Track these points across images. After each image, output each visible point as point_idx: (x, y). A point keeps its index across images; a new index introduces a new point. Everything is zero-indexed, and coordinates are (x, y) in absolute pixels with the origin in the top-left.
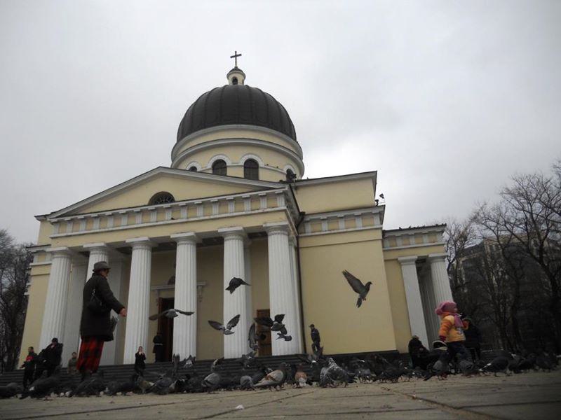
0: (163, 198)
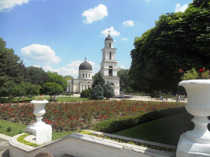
0: (89, 82)
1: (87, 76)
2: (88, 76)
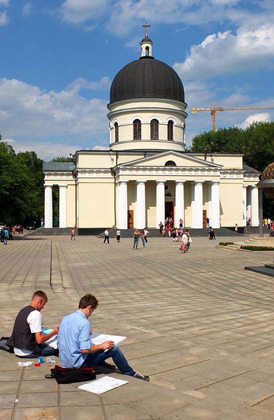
0: (170, 163)
2: (163, 131)
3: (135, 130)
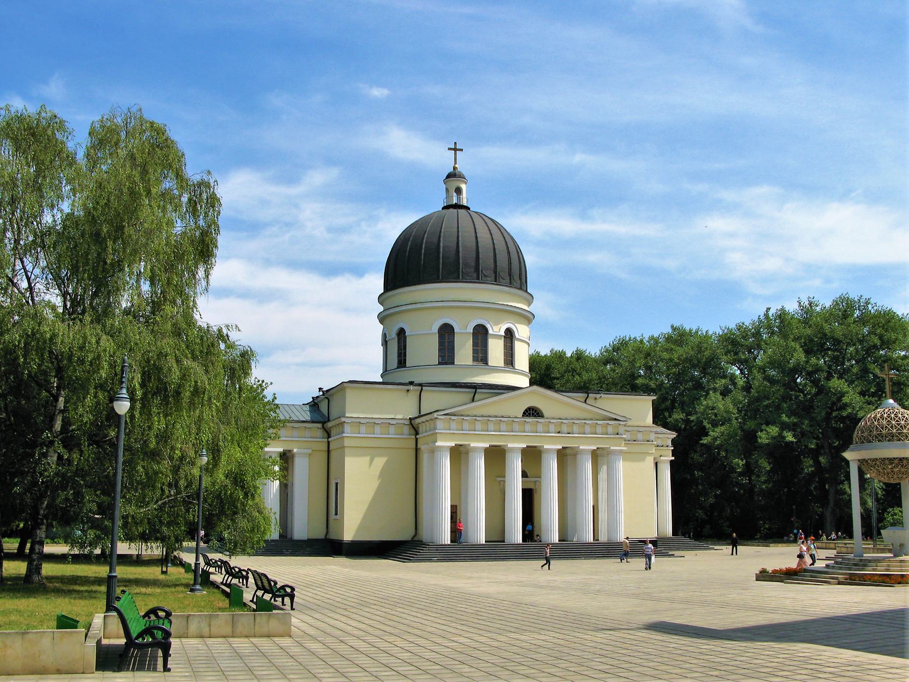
0: (532, 412)
1: (481, 355)
3: (441, 343)
